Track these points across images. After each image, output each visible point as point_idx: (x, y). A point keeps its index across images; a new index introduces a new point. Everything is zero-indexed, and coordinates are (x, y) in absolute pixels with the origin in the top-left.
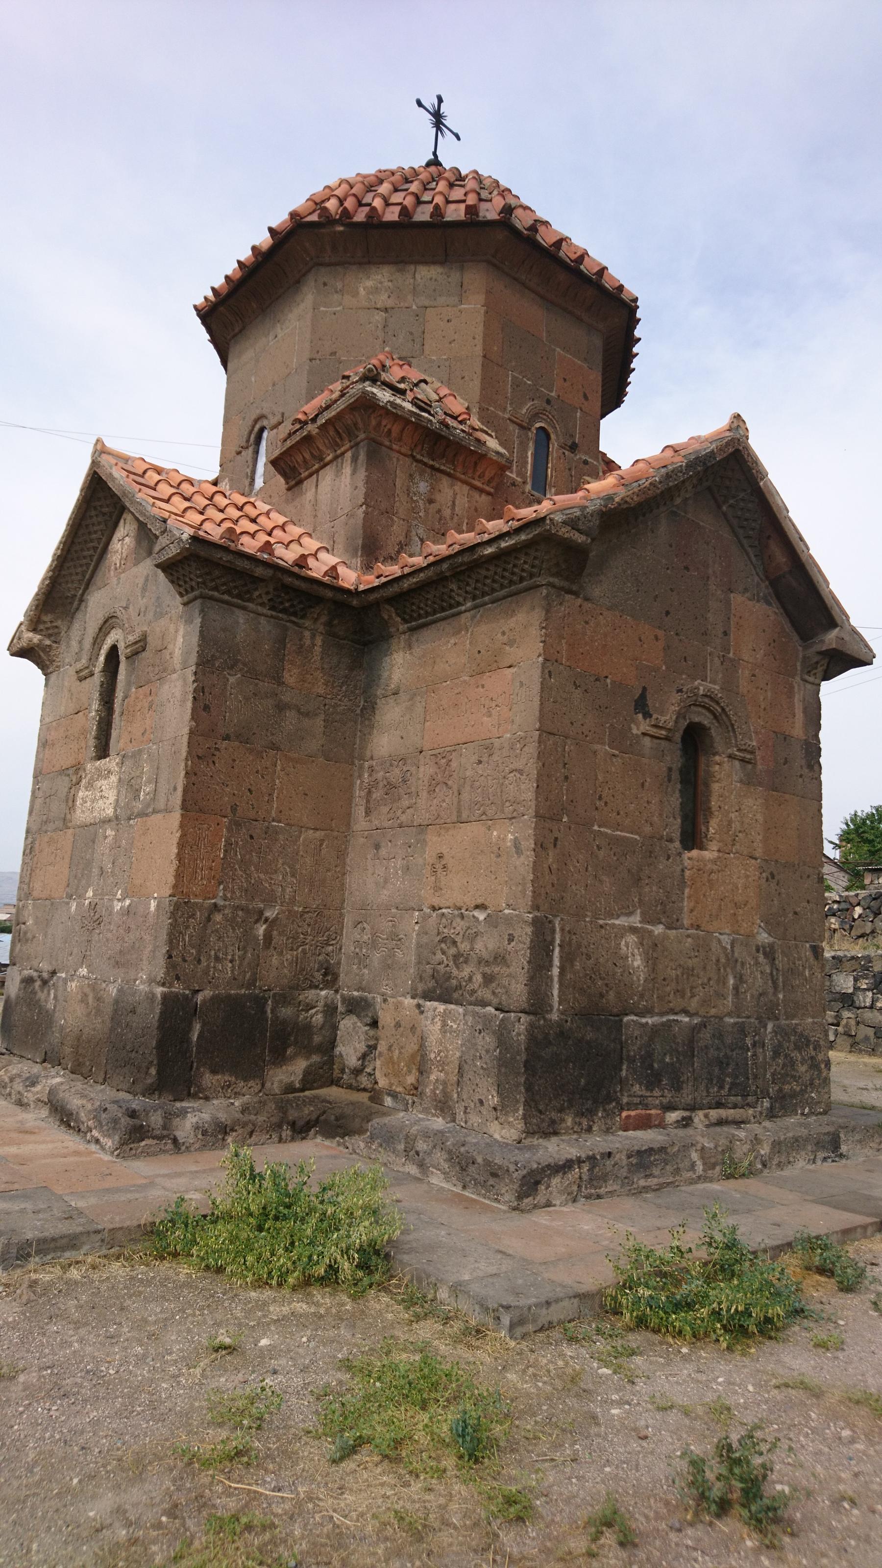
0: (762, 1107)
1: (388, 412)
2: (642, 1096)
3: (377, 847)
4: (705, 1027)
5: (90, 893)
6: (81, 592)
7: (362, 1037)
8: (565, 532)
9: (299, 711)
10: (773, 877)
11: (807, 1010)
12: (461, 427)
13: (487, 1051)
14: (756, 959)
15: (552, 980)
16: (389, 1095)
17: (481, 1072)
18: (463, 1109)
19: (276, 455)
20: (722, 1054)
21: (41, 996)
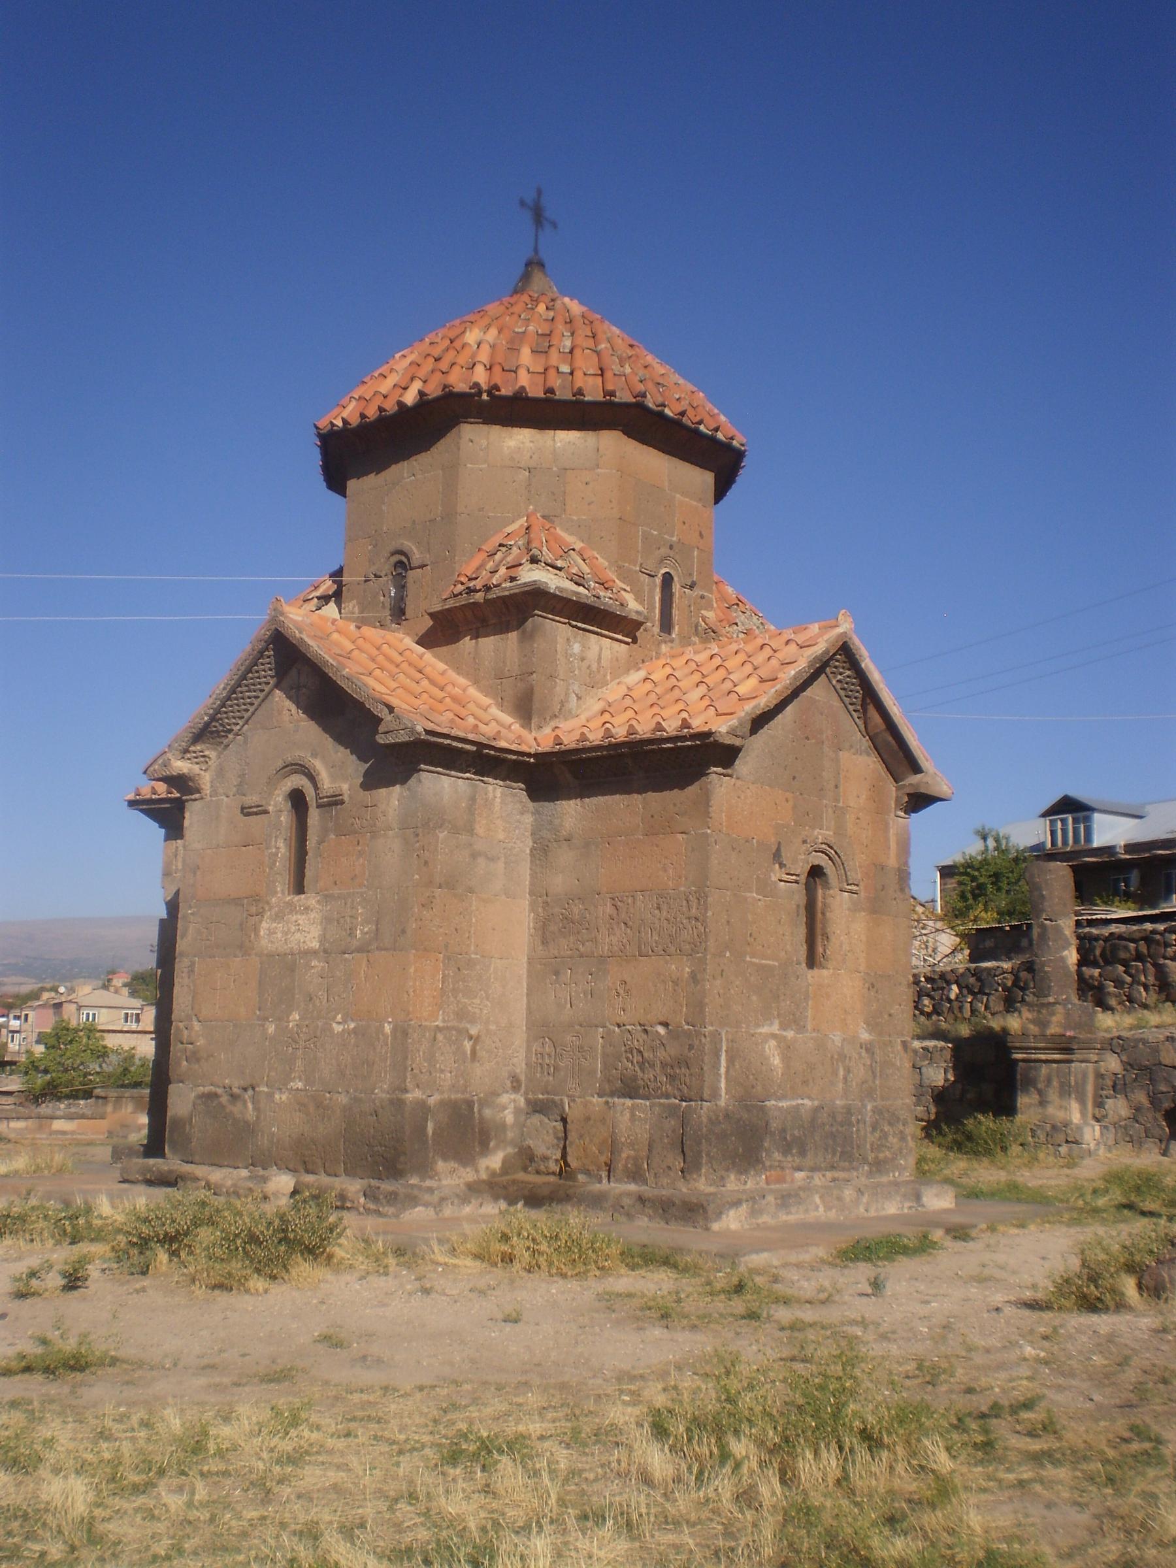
1: (554, 596)
2: (779, 1161)
3: (557, 973)
5: (296, 1016)
6: (238, 727)
7: (551, 1131)
8: (728, 741)
9: (487, 858)
10: (873, 987)
12: (609, 594)
13: (674, 1131)
14: (859, 1054)
15: (720, 1075)
18: (653, 1175)
19: (436, 610)
20: (834, 1129)
21: (236, 1109)
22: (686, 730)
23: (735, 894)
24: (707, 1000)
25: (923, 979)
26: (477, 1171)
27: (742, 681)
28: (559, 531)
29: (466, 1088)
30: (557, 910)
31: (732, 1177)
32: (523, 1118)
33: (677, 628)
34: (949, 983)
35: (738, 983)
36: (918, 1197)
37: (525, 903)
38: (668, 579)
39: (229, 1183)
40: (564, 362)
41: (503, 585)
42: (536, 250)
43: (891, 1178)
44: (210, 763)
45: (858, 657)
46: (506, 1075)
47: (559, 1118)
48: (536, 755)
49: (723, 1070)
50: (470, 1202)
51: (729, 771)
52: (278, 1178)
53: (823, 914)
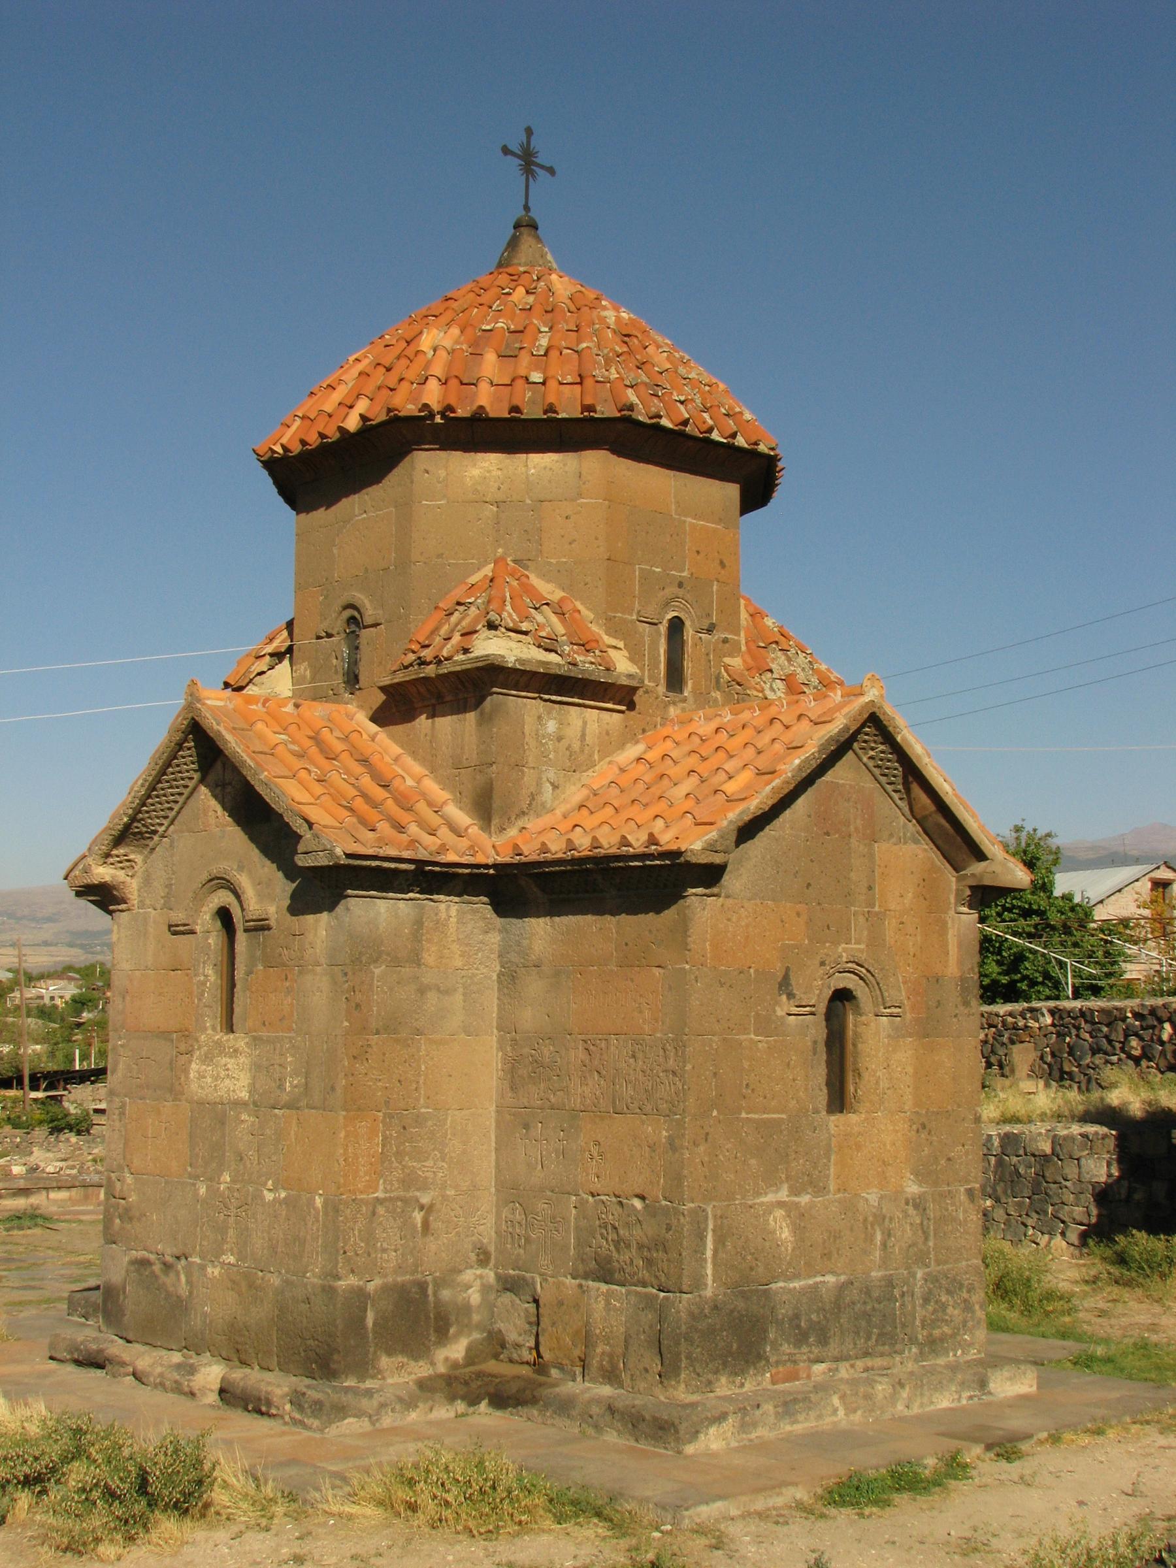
0: (909, 1352)
1: (515, 671)
2: (790, 1354)
3: (526, 1126)
4: (852, 1283)
5: (226, 1177)
6: (163, 828)
7: (522, 1314)
8: (703, 860)
11: (961, 1254)
13: (651, 1327)
14: (905, 1212)
15: (706, 1262)
16: (555, 1367)
17: (646, 1344)
18: (629, 1376)
20: (869, 1307)
22: (653, 847)
23: (724, 1039)
24: (685, 1172)
25: (1129, 1015)
26: (433, 1364)
27: (738, 772)
28: (535, 581)
29: (417, 1266)
30: (526, 1051)
31: (723, 1380)
32: (492, 1297)
33: (690, 683)
34: (1161, 1021)
35: (729, 1146)
36: (983, 1384)
37: (493, 1039)
38: (676, 626)
39: (159, 1370)
40: (536, 369)
41: (456, 658)
42: (527, 208)
43: (951, 1358)
44: (136, 868)
45: (891, 729)
46: (470, 1247)
47: (531, 1300)
48: (495, 866)
49: (709, 1253)
50: (417, 1407)
51: (715, 890)
52: (208, 1369)
53: (854, 1045)
